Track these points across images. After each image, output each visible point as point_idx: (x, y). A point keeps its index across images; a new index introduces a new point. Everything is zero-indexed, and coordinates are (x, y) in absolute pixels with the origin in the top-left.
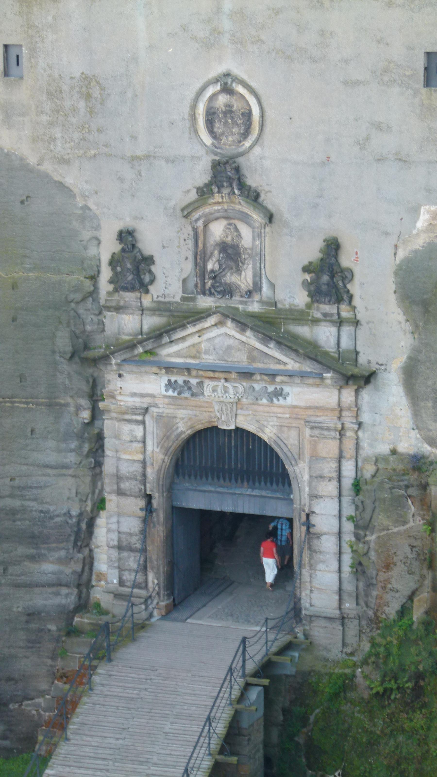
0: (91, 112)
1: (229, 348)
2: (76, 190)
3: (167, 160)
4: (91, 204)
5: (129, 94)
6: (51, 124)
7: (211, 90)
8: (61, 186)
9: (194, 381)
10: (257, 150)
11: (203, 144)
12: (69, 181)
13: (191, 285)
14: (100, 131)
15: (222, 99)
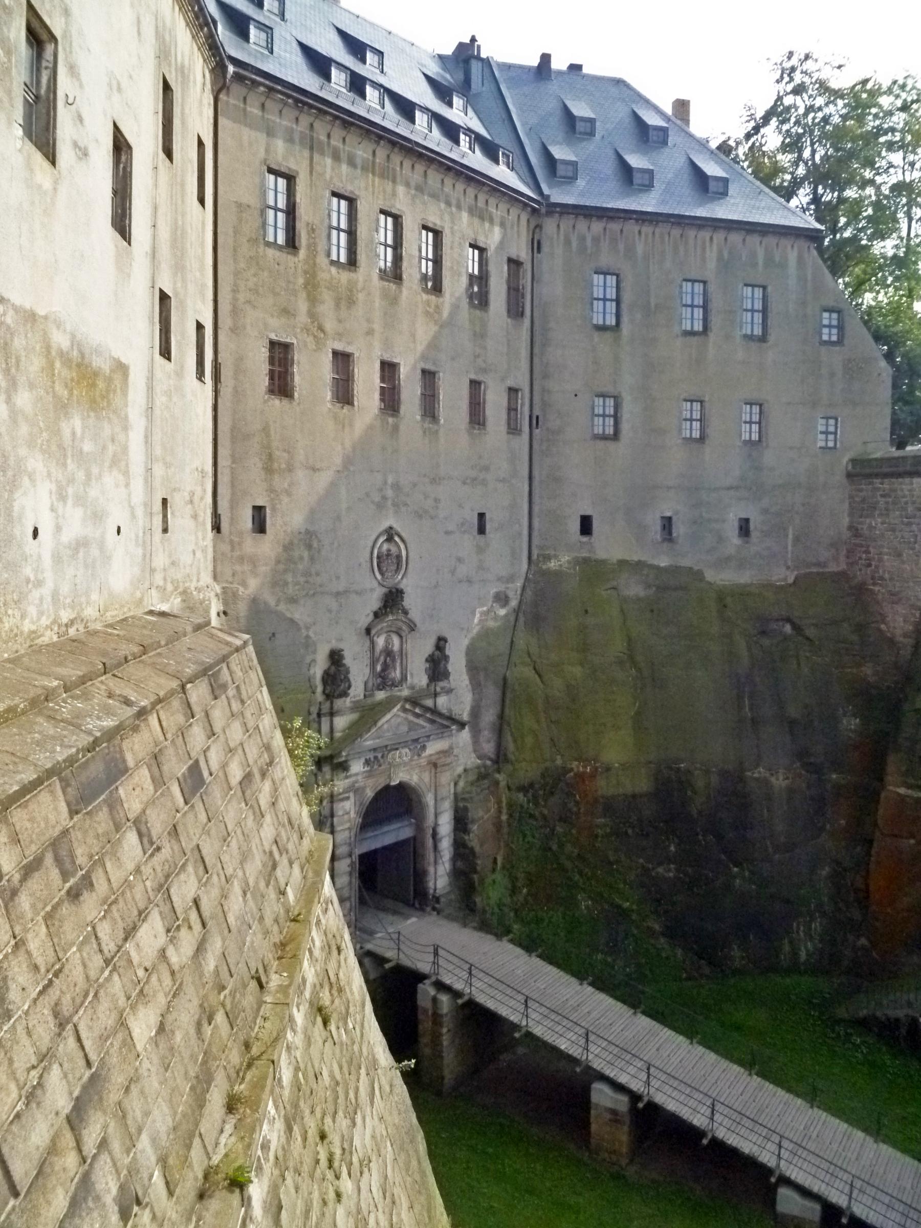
0: (312, 559)
1: (399, 724)
2: (301, 624)
3: (357, 593)
4: (311, 634)
5: (336, 544)
6: (285, 571)
7: (381, 540)
8: (292, 621)
9: (379, 755)
10: (405, 580)
11: (376, 578)
12: (297, 616)
13: (370, 684)
14: (318, 574)
15: (385, 546)
